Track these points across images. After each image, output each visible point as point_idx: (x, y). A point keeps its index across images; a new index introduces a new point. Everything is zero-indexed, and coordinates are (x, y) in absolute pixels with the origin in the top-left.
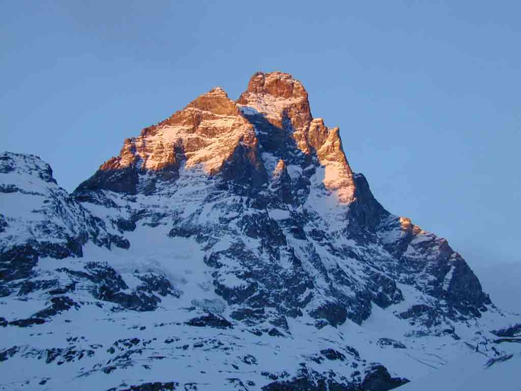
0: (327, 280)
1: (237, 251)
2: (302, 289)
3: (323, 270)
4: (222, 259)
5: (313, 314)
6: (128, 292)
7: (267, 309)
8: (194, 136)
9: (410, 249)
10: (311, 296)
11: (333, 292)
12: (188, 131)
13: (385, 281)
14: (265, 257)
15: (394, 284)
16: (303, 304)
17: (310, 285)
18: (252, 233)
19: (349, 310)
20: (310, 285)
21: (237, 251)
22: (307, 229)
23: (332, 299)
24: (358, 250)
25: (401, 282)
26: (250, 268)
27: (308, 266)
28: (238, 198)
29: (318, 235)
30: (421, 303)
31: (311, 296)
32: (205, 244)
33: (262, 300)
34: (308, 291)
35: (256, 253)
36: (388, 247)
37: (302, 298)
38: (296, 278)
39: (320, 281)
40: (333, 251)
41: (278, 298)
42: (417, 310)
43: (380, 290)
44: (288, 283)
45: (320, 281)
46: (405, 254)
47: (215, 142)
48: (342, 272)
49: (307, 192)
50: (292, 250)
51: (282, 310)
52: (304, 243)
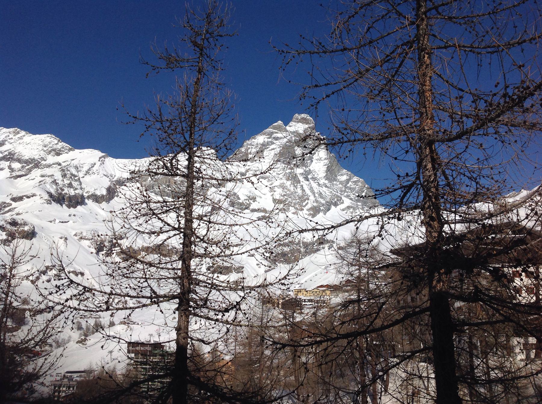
0: (315, 196)
1: (282, 186)
2: (305, 200)
3: (314, 193)
4: (276, 189)
5: (307, 210)
6: (240, 201)
7: (291, 208)
8: (270, 140)
9: (350, 183)
10: (308, 203)
11: (317, 201)
12: (268, 138)
13: (338, 196)
14: (292, 188)
15: (341, 198)
16: (305, 206)
17: (308, 199)
18: (288, 179)
19: (322, 208)
20: (308, 199)
21: (282, 186)
22: (309, 177)
23: (315, 204)
24: (328, 185)
25: (345, 196)
26: (286, 192)
27: (308, 192)
28: (284, 165)
29: (314, 179)
30: (351, 205)
31: (308, 203)
32: (271, 183)
33: (289, 205)
34: (307, 201)
35: (289, 186)
36: (341, 183)
37: (304, 204)
38: (303, 196)
39: (312, 198)
40: (319, 185)
41: (295, 204)
42: (349, 207)
43: (336, 200)
44: (300, 198)
45: (312, 198)
46: (348, 185)
47: (278, 142)
48: (321, 193)
49: (312, 161)
50: (302, 186)
51: (297, 209)
52: (307, 183)
